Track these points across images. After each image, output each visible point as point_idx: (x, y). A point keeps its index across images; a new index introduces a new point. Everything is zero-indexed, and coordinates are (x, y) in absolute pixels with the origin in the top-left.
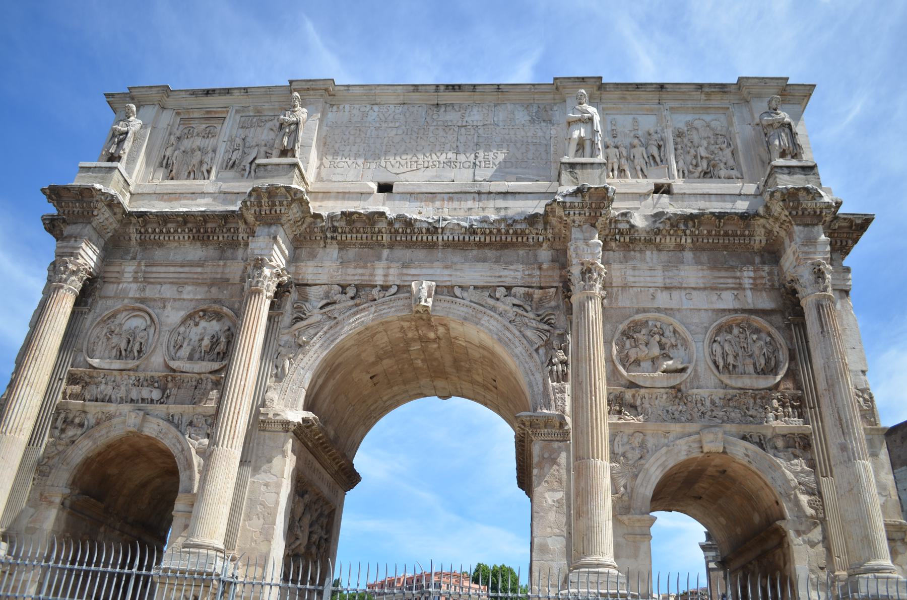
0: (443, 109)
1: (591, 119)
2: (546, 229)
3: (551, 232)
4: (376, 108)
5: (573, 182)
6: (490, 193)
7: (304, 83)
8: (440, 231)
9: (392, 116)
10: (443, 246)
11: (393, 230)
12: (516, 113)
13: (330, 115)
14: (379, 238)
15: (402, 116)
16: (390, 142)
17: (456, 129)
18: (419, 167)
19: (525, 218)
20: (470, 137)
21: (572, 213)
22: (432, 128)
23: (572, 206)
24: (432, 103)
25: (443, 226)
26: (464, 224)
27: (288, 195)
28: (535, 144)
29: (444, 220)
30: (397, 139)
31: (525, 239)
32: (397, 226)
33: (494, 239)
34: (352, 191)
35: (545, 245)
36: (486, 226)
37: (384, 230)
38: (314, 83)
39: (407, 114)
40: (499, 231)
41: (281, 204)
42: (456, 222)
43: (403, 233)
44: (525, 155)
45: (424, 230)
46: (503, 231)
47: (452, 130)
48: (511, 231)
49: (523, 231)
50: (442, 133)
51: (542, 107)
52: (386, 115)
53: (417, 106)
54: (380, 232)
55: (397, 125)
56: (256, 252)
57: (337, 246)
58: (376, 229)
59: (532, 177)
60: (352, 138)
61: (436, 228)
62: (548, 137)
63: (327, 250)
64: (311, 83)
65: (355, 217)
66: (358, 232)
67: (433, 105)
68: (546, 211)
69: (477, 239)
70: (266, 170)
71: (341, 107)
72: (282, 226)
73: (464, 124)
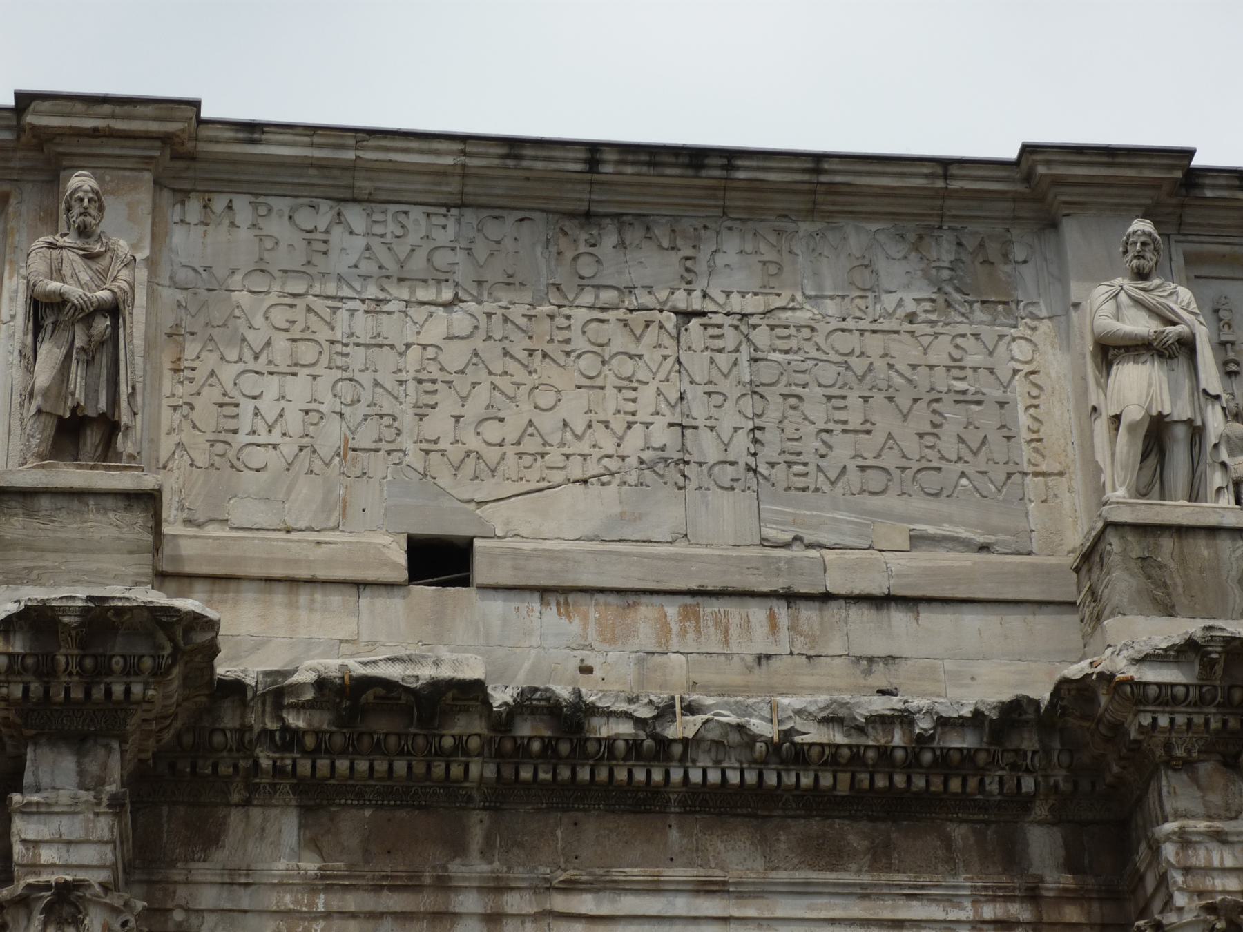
0: (610, 239)
1: (1187, 346)
2: (1047, 751)
3: (1065, 759)
4: (355, 216)
5: (1155, 600)
6: (826, 597)
7: (79, 107)
8: (677, 749)
9: (421, 255)
10: (682, 803)
11: (508, 745)
12: (881, 265)
13: (178, 236)
14: (456, 771)
15: (460, 256)
16: (433, 368)
17: (670, 320)
18: (558, 477)
19: (977, 713)
20: (723, 360)
21: (1163, 721)
22: (581, 315)
23: (1165, 696)
24: (570, 207)
25: (690, 734)
26: (759, 726)
27: (162, 637)
28: (962, 399)
29: (690, 709)
30: (456, 355)
31: (973, 783)
32: (524, 729)
33: (866, 784)
34: (322, 574)
35: (1041, 810)
36: (840, 739)
37: (474, 743)
38: (118, 110)
39: (481, 252)
40: (885, 753)
41: (132, 670)
42: (733, 719)
43: (543, 754)
44: (929, 440)
45: (621, 744)
46: (899, 754)
47: (654, 328)
48: (927, 757)
49: (968, 755)
50: (621, 341)
51: (971, 244)
52: (402, 250)
53: (511, 217)
54: (460, 747)
55: (447, 295)
56: (47, 855)
57: (292, 799)
58: (448, 742)
59: (963, 533)
60: (281, 343)
61: (663, 744)
62: (1004, 373)
63: (256, 813)
64: (107, 108)
65: (369, 696)
66: (378, 748)
67: (571, 215)
68: (1056, 693)
69: (806, 781)
70: (30, 514)
71: (219, 203)
72: (123, 740)
73: (697, 305)
